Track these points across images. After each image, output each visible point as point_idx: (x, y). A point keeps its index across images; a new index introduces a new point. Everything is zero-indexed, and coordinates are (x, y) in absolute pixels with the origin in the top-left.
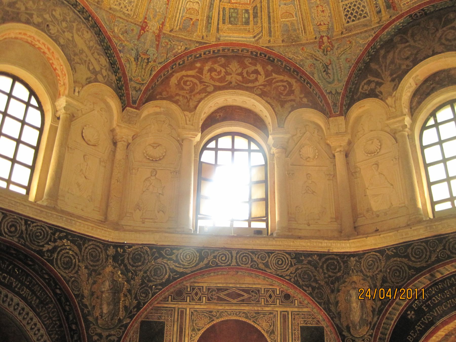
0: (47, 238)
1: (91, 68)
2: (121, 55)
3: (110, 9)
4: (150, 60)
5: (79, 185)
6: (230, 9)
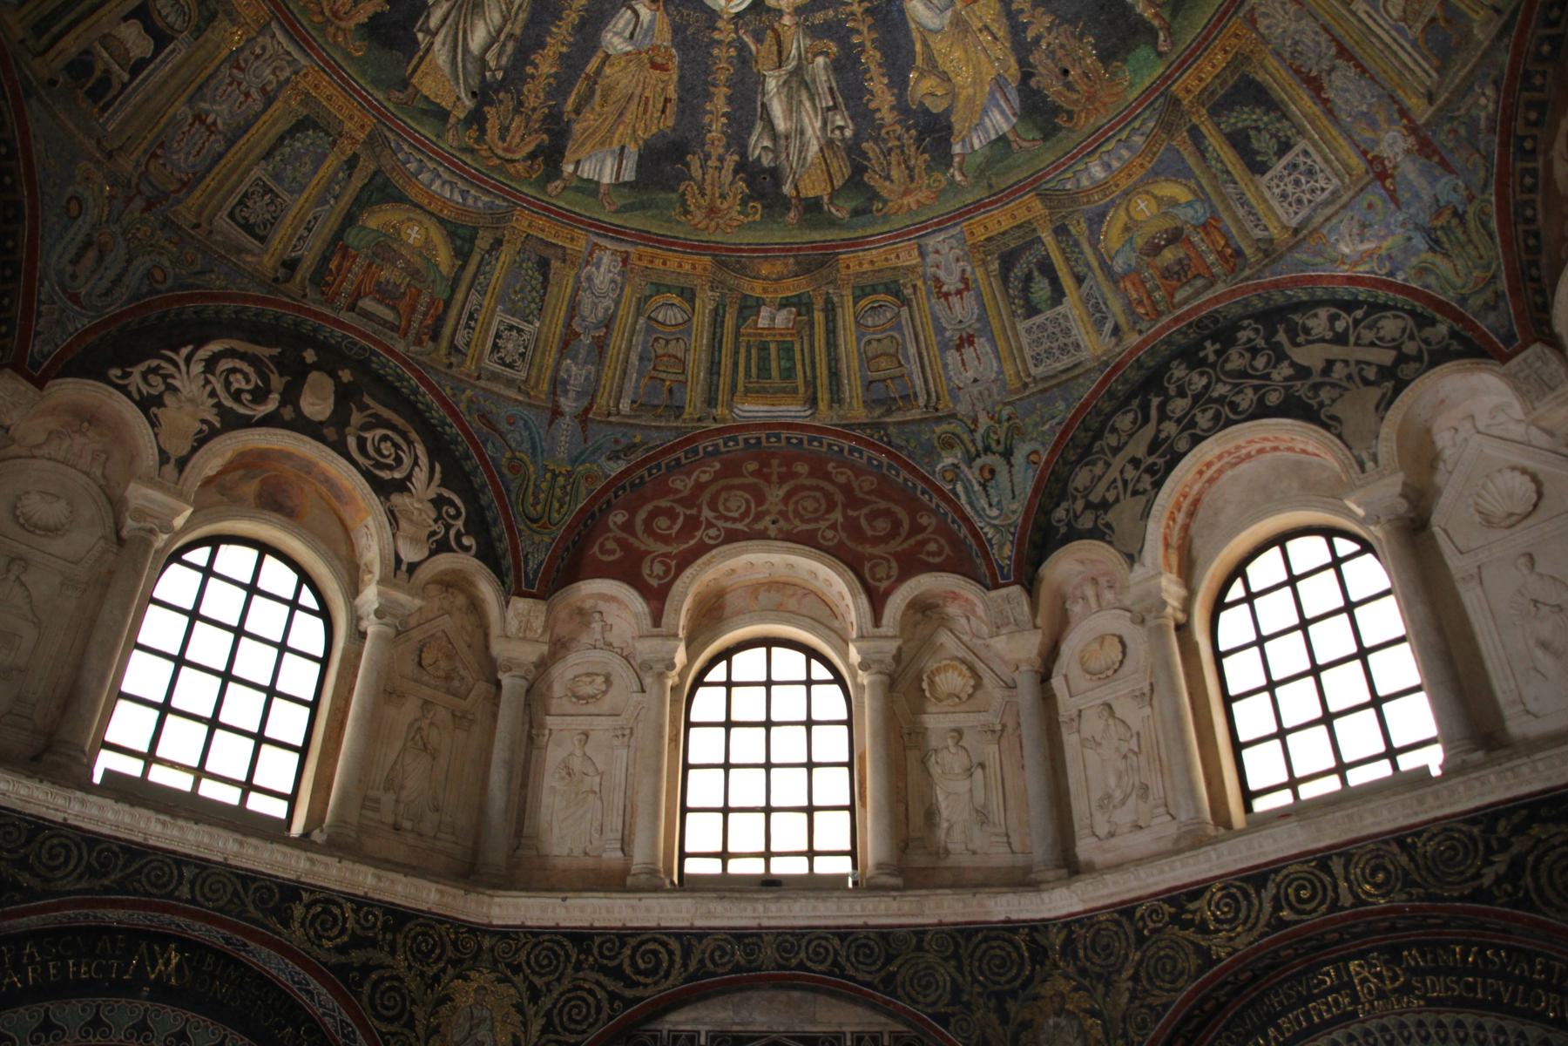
0: (1476, 851)
1: (1371, 374)
2: (1400, 278)
3: (1296, 231)
4: (1460, 211)
5: (1544, 645)
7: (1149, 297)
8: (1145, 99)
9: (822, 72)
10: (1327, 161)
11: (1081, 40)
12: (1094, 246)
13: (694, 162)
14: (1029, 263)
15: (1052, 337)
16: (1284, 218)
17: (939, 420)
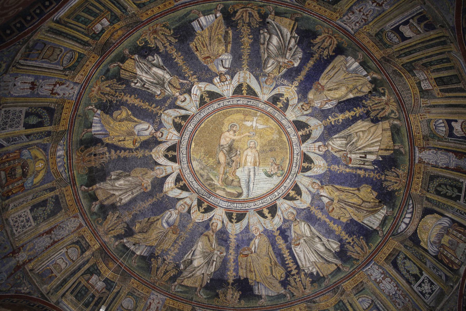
3: (7, 220)
6: (84, 286)
7: (8, 161)
8: (72, 177)
9: (155, 91)
10: (25, 233)
11: (100, 164)
12: (35, 144)
13: (173, 40)
14: (45, 118)
15: (13, 120)
16: (13, 216)
17: (8, 67)
